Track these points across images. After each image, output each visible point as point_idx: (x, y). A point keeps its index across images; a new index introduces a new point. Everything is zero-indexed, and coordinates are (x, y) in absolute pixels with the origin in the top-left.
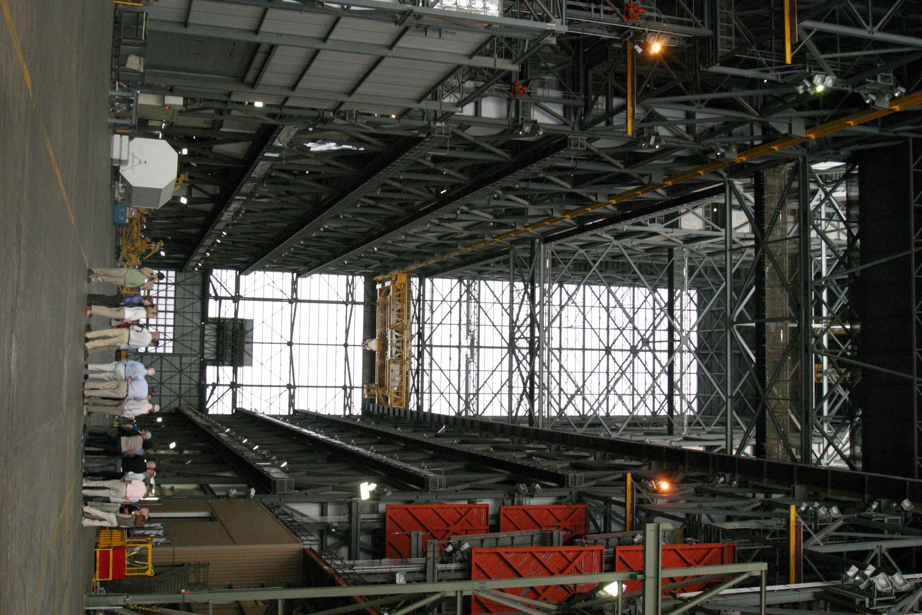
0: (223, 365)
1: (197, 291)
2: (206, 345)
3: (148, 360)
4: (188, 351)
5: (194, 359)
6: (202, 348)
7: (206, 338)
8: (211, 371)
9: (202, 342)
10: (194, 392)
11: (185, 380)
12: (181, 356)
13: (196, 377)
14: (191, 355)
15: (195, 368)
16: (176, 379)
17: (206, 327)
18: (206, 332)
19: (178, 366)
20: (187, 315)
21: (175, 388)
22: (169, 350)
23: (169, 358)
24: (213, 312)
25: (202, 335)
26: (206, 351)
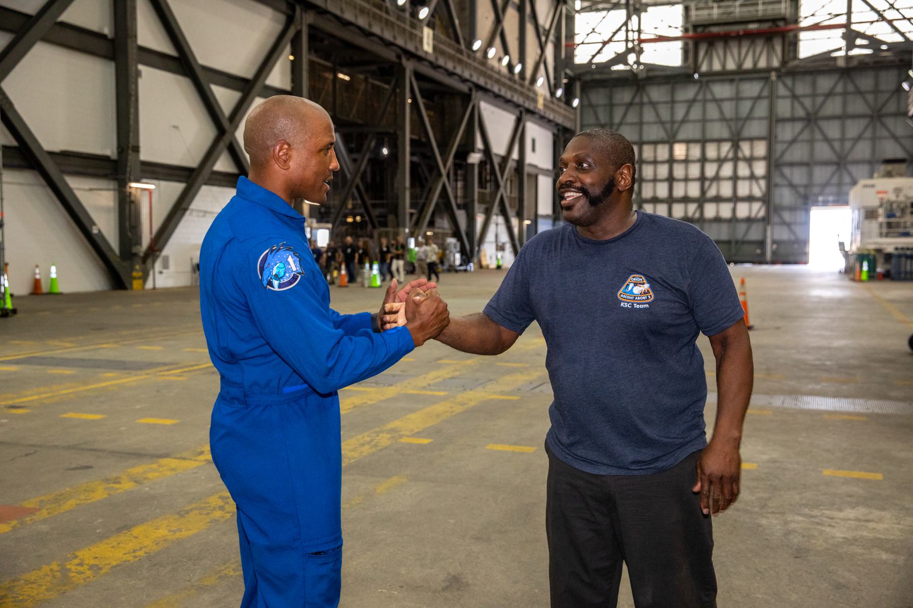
0: (796, 21)
1: (625, 95)
2: (748, 64)
3: (785, 196)
4: (762, 109)
5: (782, 90)
6: (755, 74)
7: (731, 65)
8: (810, 46)
9: (739, 75)
10: (866, 82)
11: (834, 106)
12: (774, 120)
13: (825, 83)
14: (772, 98)
15: (802, 88)
16: (833, 130)
17: (704, 68)
18: (717, 67)
19: (799, 126)
20: (680, 113)
21: (854, 128)
22: (761, 149)
23: (779, 148)
24: (669, 56)
25: (725, 76)
26: (762, 64)
